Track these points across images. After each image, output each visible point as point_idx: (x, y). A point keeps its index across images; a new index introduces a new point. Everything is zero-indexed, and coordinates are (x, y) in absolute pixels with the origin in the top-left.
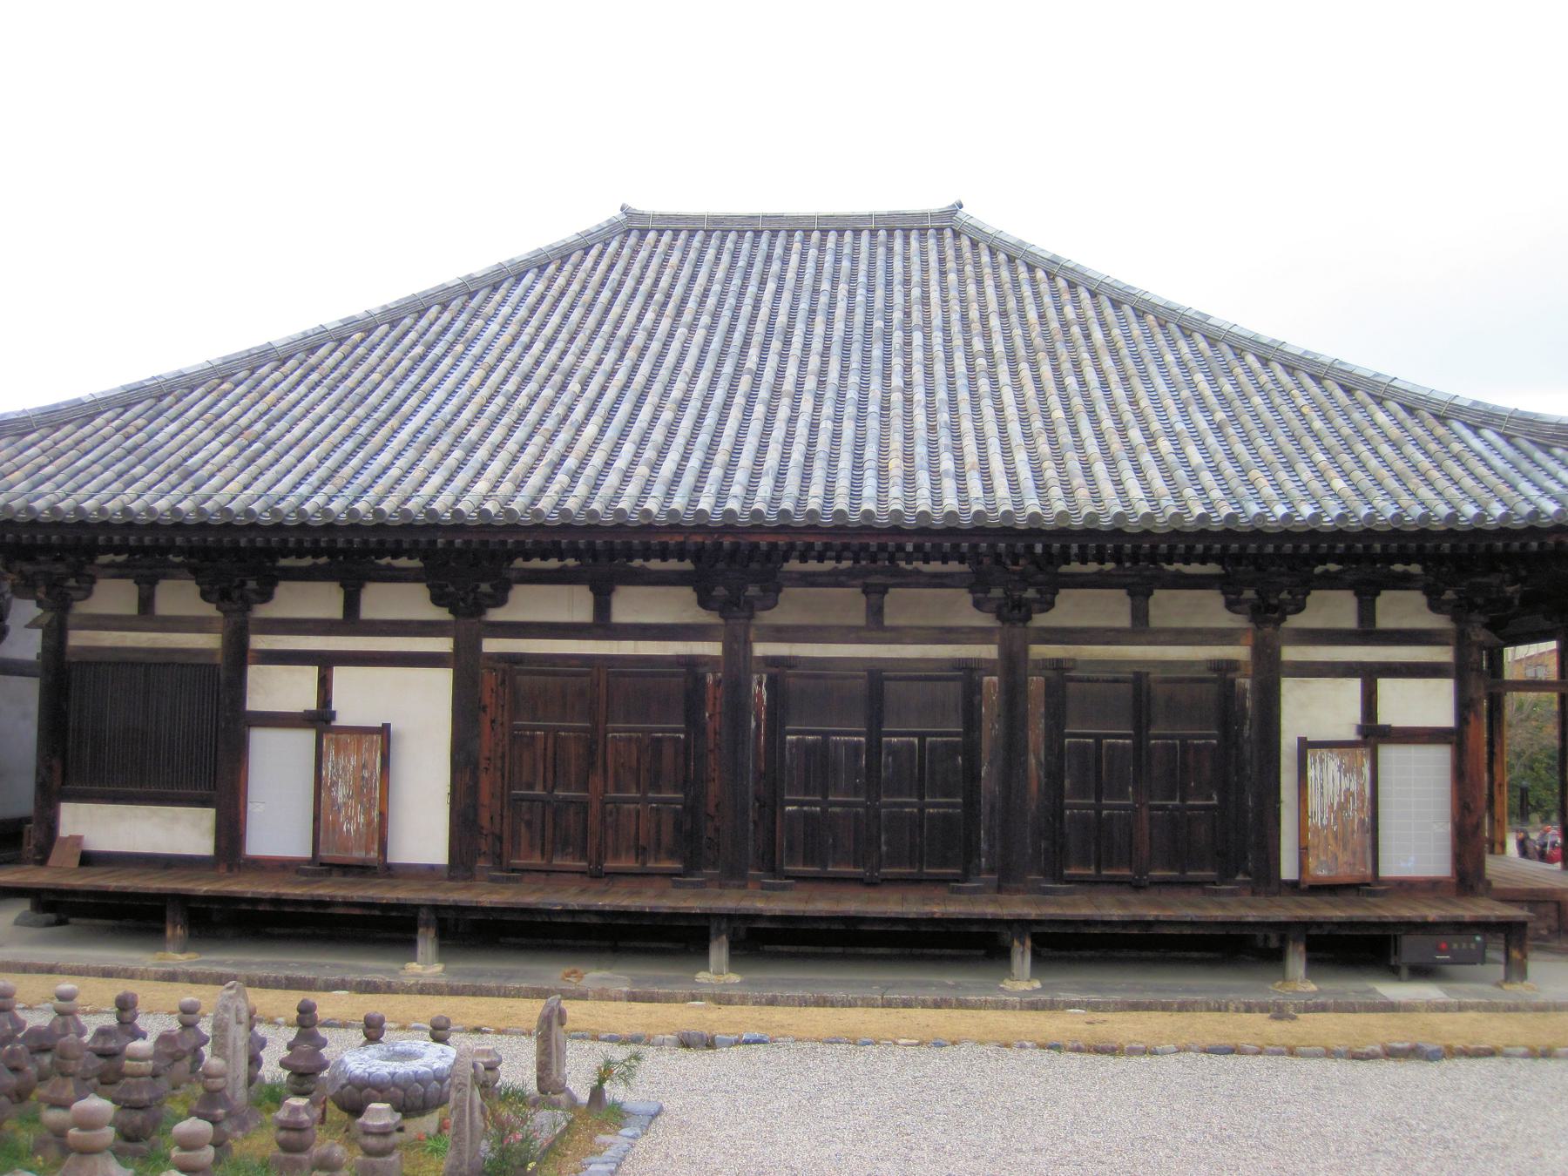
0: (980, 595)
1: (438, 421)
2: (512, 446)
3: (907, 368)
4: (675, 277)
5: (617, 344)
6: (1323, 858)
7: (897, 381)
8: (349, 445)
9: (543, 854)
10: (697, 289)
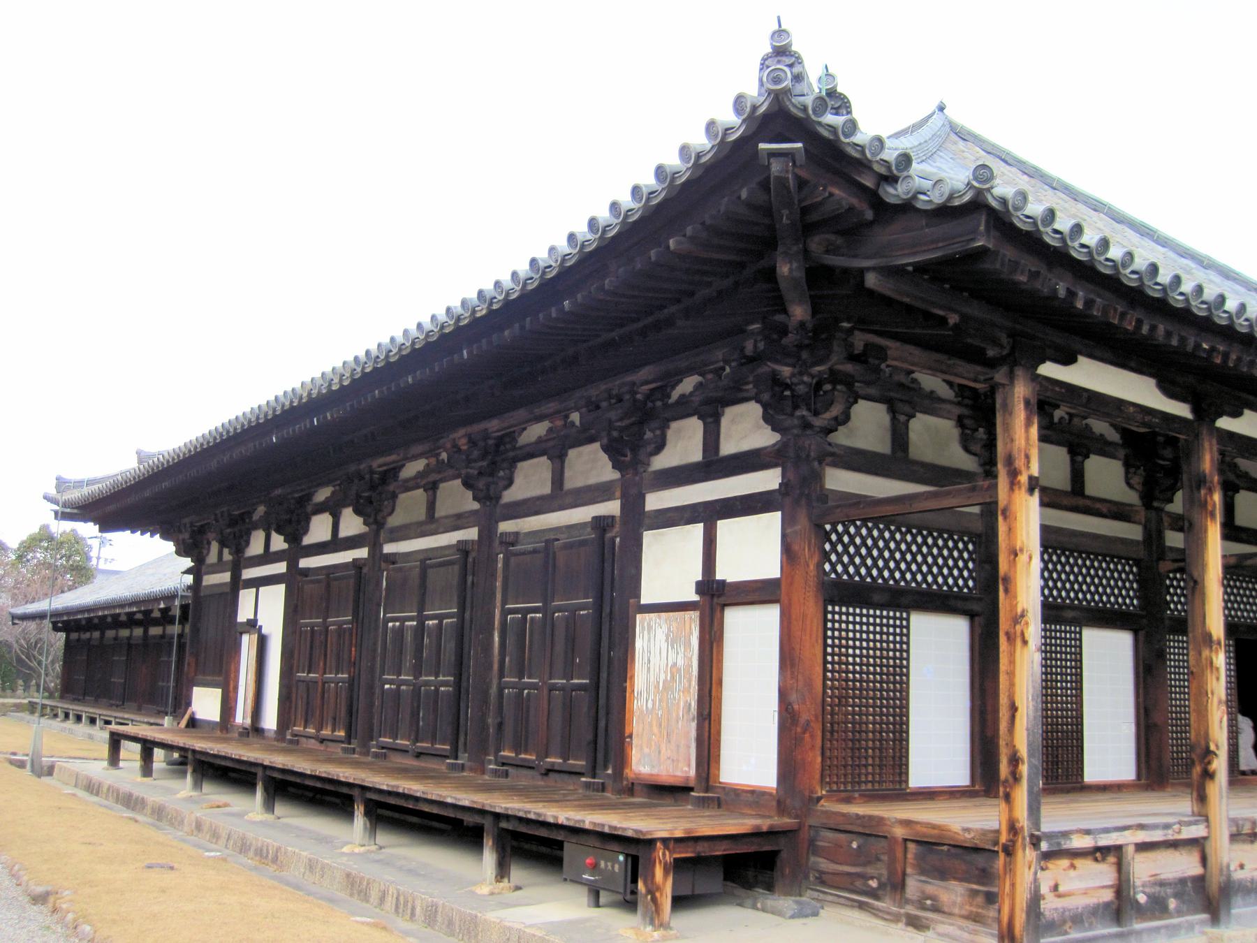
6: (646, 750)
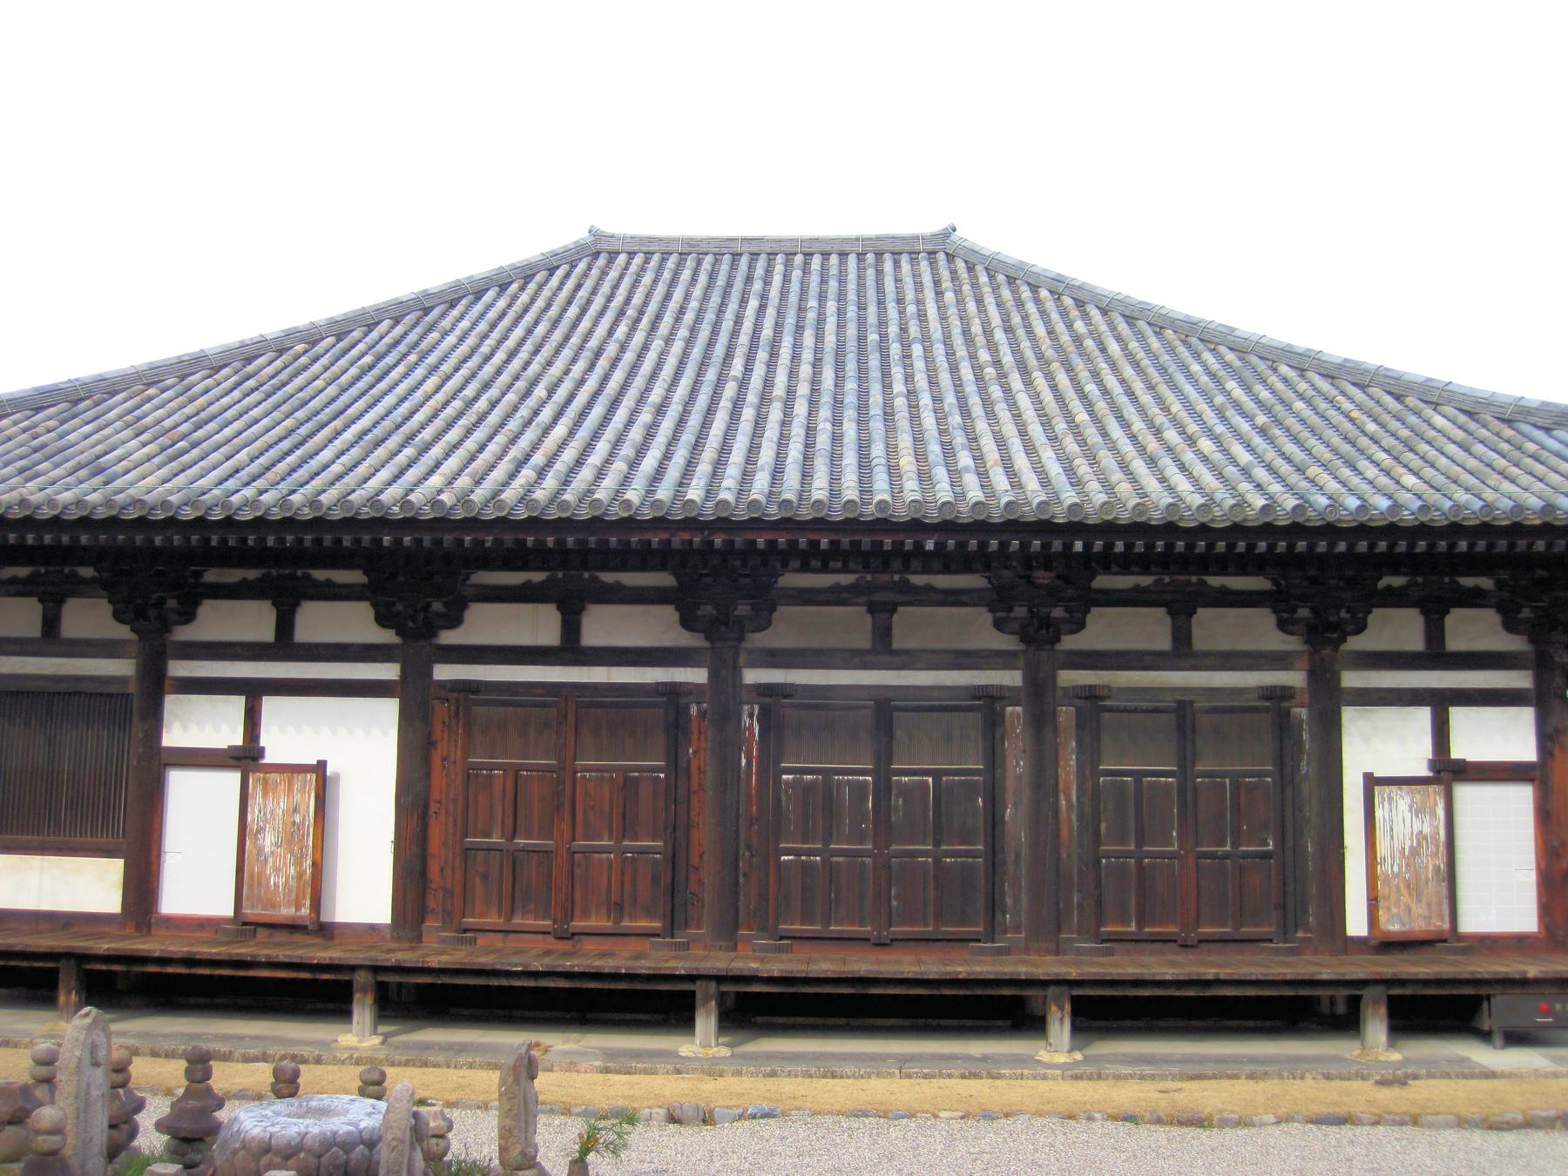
0: (1001, 614)
1: (387, 423)
2: (471, 444)
3: (909, 378)
4: (648, 296)
5: (586, 355)
6: (1395, 910)
7: (899, 387)
8: (286, 445)
9: (500, 912)
10: (673, 305)
